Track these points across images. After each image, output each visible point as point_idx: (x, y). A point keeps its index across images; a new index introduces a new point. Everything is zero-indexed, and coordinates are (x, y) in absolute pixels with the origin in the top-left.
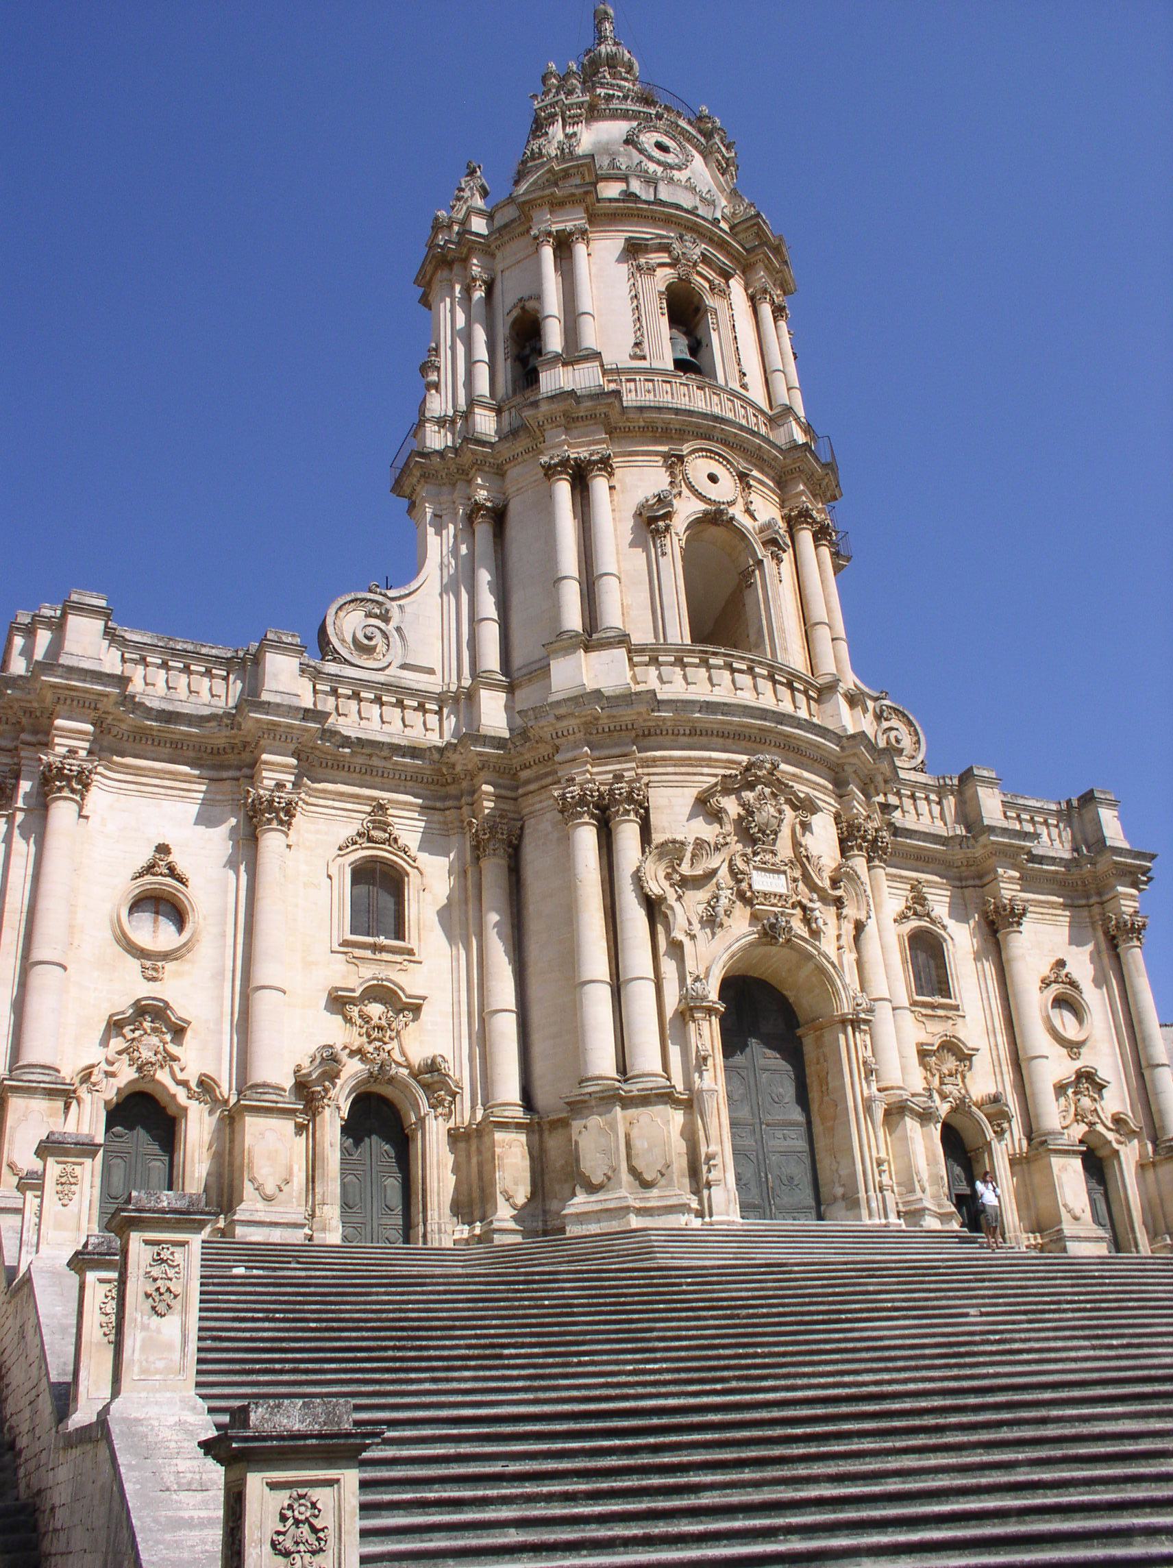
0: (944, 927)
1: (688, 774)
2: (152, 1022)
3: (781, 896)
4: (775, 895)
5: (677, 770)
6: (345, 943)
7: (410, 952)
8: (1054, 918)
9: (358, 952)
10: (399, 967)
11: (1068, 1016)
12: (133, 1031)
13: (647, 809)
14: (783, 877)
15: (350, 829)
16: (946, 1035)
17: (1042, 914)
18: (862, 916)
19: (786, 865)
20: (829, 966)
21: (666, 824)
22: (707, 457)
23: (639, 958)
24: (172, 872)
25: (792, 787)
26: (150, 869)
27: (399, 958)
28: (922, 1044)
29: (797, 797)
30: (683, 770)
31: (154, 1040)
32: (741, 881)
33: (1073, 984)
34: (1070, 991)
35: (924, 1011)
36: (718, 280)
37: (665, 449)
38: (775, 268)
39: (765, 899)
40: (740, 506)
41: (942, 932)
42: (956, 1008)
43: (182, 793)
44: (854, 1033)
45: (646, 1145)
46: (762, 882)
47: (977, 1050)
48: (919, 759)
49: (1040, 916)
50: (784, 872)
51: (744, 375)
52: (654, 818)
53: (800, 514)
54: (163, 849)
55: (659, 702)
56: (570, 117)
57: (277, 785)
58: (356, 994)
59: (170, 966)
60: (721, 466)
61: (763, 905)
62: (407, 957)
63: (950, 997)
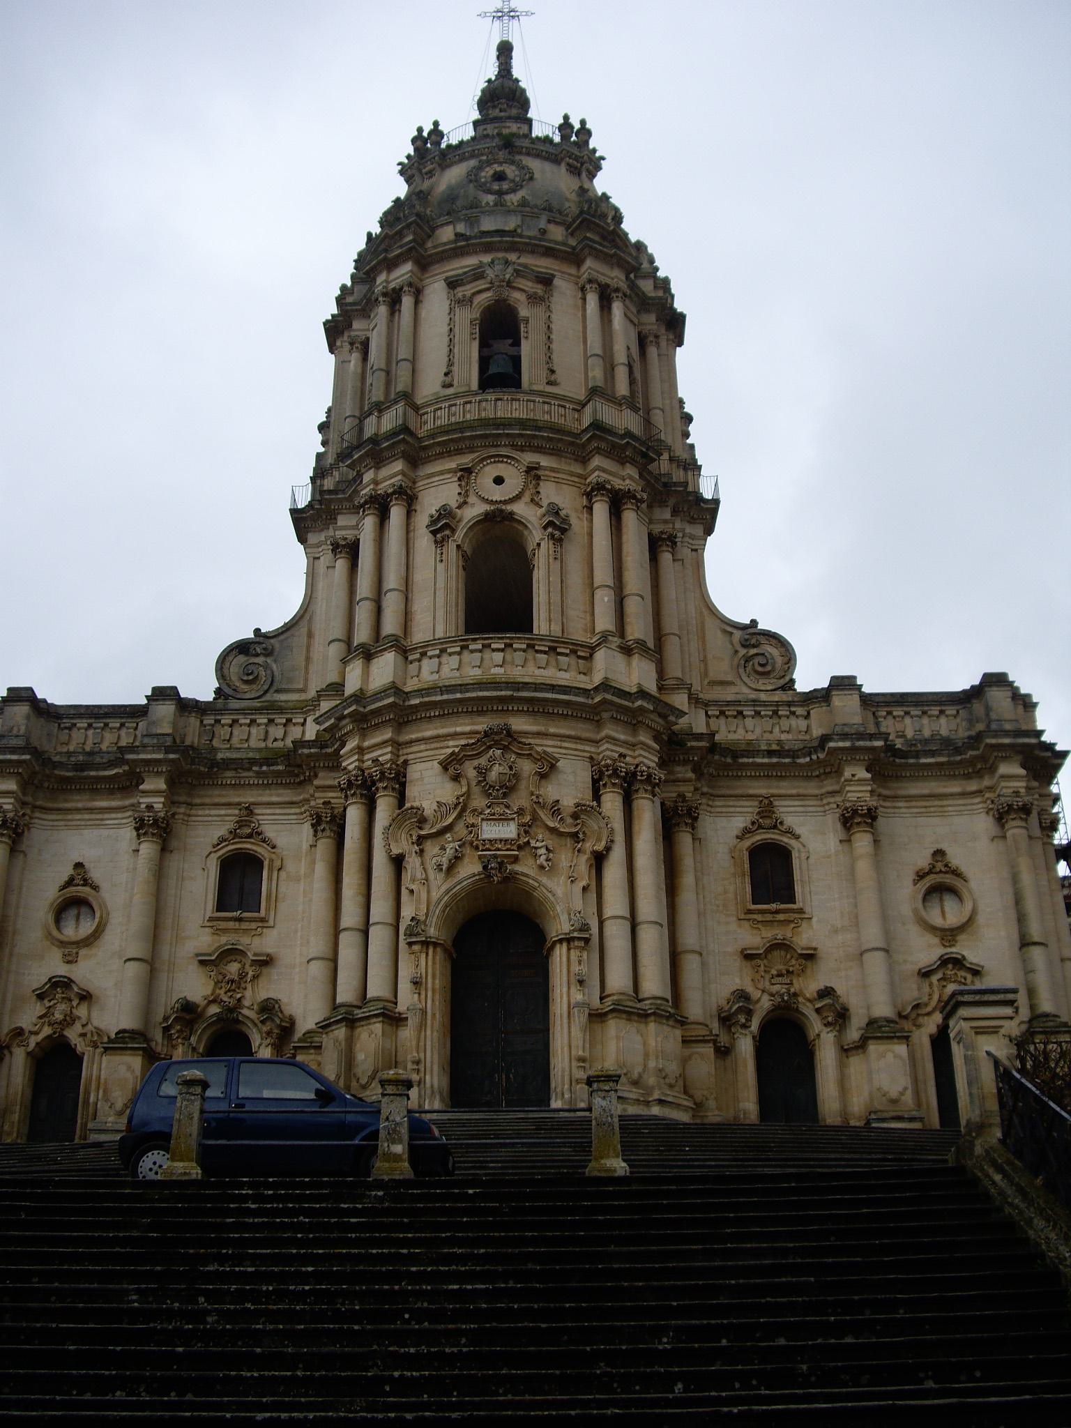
0: (797, 837)
1: (437, 749)
2: (63, 993)
3: (506, 841)
4: (501, 840)
5: (428, 747)
6: (211, 919)
7: (263, 920)
8: (940, 809)
9: (223, 925)
10: (253, 933)
11: (950, 903)
12: (50, 1001)
13: (403, 785)
14: (511, 823)
15: (222, 831)
16: (776, 939)
17: (926, 807)
18: (600, 847)
19: (515, 813)
20: (550, 895)
21: (416, 794)
22: (495, 462)
23: (380, 909)
24: (86, 882)
25: (529, 744)
26: (70, 882)
27: (254, 925)
28: (746, 949)
29: (538, 753)
30: (433, 746)
31: (62, 1007)
32: (471, 832)
33: (956, 873)
34: (948, 879)
35: (759, 917)
36: (539, 289)
37: (453, 465)
38: (606, 254)
39: (492, 845)
40: (527, 498)
41: (793, 843)
42: (801, 911)
43: (97, 822)
44: (569, 949)
45: (363, 1057)
46: (491, 831)
47: (815, 949)
48: (787, 679)
49: (923, 810)
50: (513, 819)
51: (553, 372)
52: (411, 791)
53: (592, 490)
54: (79, 865)
55: (407, 693)
56: (426, 174)
57: (147, 807)
58: (213, 958)
59: (83, 952)
60: (510, 467)
61: (490, 850)
62: (260, 924)
63: (795, 903)
